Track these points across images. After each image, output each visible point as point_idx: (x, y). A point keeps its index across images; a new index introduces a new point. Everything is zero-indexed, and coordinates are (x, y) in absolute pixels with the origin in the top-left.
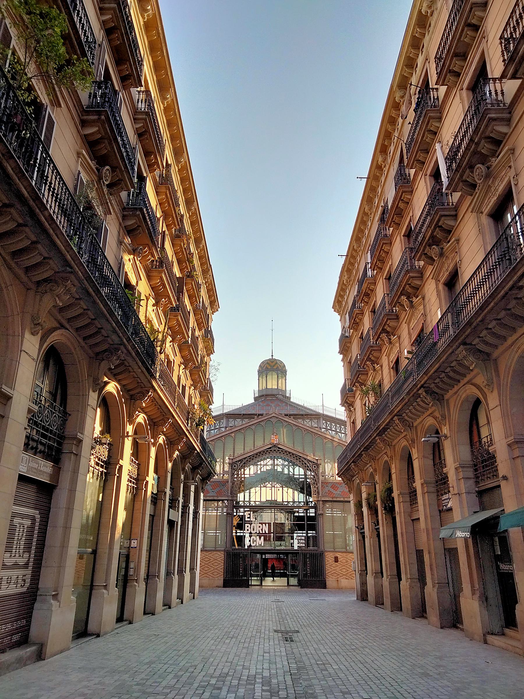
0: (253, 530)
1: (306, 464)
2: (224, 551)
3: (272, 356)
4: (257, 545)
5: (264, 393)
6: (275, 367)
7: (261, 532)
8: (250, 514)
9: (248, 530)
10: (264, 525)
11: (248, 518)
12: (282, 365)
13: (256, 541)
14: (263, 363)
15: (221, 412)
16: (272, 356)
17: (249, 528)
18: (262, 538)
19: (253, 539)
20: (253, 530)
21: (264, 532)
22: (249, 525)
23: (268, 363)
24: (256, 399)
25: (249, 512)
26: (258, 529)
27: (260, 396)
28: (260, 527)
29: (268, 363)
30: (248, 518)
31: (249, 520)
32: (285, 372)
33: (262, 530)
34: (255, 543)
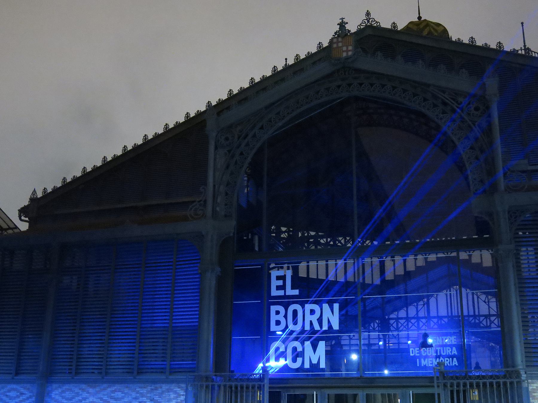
1: (445, 104)
3: (419, 18)
4: (307, 366)
7: (317, 327)
8: (282, 278)
10: (326, 306)
11: (278, 288)
12: (440, 29)
13: (301, 354)
17: (281, 317)
18: (322, 345)
19: (295, 349)
21: (325, 327)
22: (281, 309)
25: (281, 273)
26: (309, 317)
28: (312, 312)
30: (278, 288)
31: (281, 293)
33: (320, 320)
34: (299, 360)
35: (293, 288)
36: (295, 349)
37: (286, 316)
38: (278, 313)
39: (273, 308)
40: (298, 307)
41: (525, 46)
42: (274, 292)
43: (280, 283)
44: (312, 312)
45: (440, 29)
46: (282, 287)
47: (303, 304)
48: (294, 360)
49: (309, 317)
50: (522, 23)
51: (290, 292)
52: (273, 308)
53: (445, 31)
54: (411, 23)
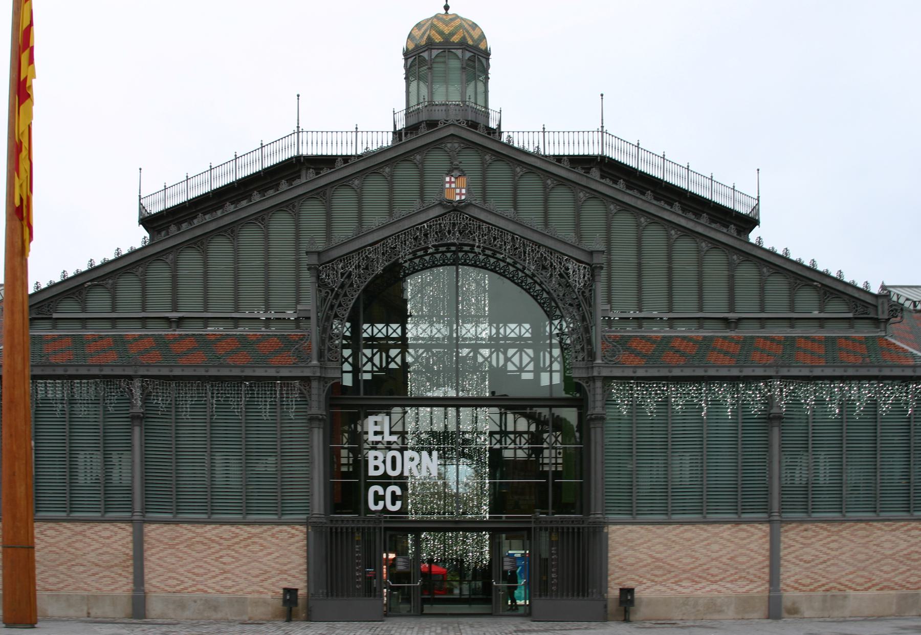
0: (394, 468)
2: (306, 523)
3: (447, 8)
5: (424, 117)
6: (456, 39)
9: (376, 468)
10: (425, 454)
11: (376, 433)
14: (419, 26)
15: (292, 153)
16: (447, 8)
17: (379, 463)
19: (393, 493)
20: (394, 468)
23: (433, 26)
24: (397, 134)
27: (411, 129)
29: (433, 26)
30: (376, 433)
32: (487, 54)
35: (391, 433)
36: (393, 493)
37: (384, 462)
38: (376, 458)
39: (371, 454)
40: (397, 454)
41: (602, 127)
42: (371, 438)
43: (378, 429)
44: (412, 459)
45: (476, 35)
46: (381, 433)
47: (402, 450)
48: (393, 504)
49: (408, 465)
50: (602, 95)
51: (388, 438)
52: (371, 454)
53: (482, 37)
54: (436, 17)
